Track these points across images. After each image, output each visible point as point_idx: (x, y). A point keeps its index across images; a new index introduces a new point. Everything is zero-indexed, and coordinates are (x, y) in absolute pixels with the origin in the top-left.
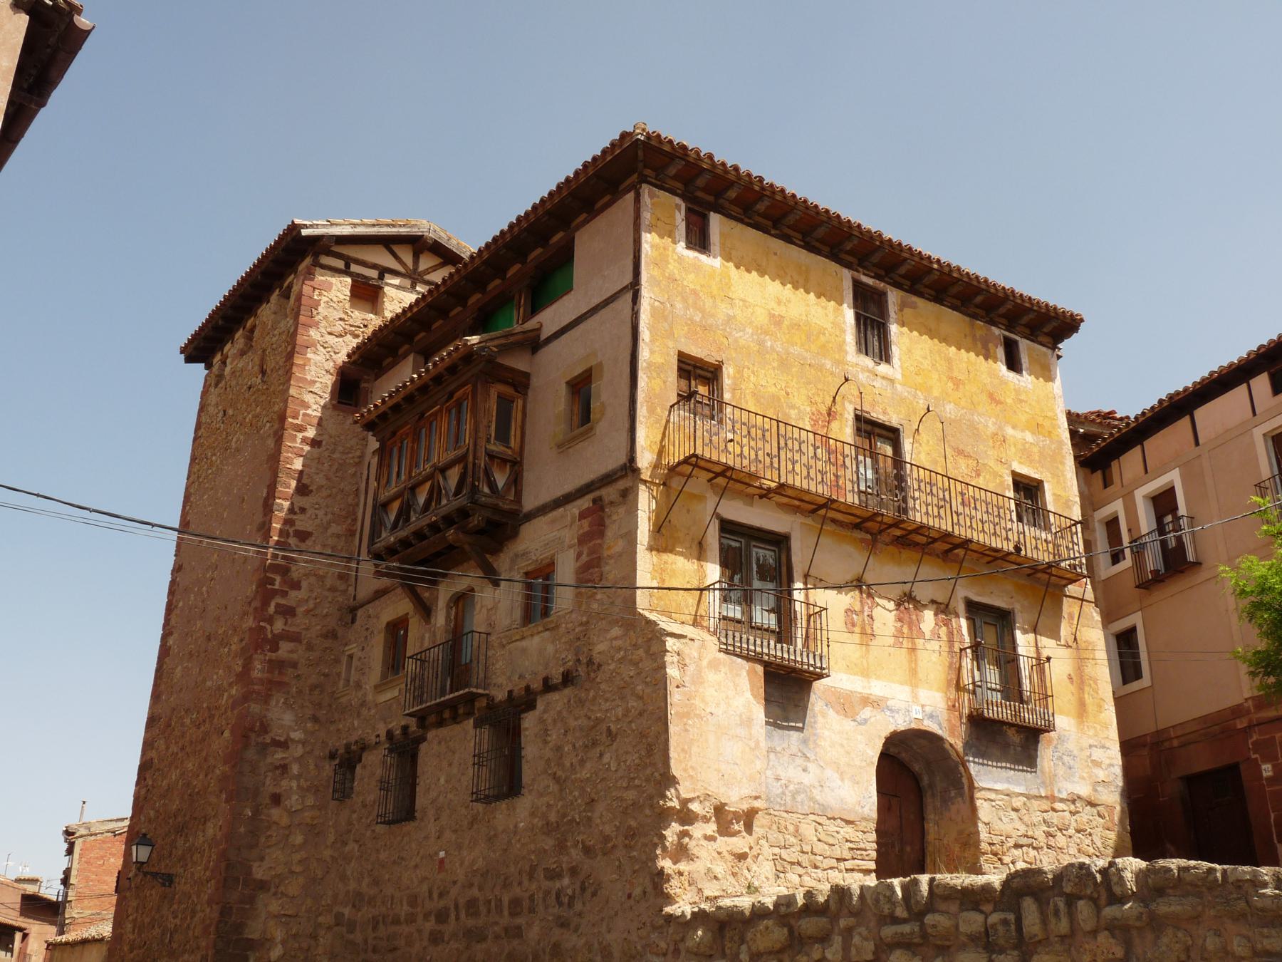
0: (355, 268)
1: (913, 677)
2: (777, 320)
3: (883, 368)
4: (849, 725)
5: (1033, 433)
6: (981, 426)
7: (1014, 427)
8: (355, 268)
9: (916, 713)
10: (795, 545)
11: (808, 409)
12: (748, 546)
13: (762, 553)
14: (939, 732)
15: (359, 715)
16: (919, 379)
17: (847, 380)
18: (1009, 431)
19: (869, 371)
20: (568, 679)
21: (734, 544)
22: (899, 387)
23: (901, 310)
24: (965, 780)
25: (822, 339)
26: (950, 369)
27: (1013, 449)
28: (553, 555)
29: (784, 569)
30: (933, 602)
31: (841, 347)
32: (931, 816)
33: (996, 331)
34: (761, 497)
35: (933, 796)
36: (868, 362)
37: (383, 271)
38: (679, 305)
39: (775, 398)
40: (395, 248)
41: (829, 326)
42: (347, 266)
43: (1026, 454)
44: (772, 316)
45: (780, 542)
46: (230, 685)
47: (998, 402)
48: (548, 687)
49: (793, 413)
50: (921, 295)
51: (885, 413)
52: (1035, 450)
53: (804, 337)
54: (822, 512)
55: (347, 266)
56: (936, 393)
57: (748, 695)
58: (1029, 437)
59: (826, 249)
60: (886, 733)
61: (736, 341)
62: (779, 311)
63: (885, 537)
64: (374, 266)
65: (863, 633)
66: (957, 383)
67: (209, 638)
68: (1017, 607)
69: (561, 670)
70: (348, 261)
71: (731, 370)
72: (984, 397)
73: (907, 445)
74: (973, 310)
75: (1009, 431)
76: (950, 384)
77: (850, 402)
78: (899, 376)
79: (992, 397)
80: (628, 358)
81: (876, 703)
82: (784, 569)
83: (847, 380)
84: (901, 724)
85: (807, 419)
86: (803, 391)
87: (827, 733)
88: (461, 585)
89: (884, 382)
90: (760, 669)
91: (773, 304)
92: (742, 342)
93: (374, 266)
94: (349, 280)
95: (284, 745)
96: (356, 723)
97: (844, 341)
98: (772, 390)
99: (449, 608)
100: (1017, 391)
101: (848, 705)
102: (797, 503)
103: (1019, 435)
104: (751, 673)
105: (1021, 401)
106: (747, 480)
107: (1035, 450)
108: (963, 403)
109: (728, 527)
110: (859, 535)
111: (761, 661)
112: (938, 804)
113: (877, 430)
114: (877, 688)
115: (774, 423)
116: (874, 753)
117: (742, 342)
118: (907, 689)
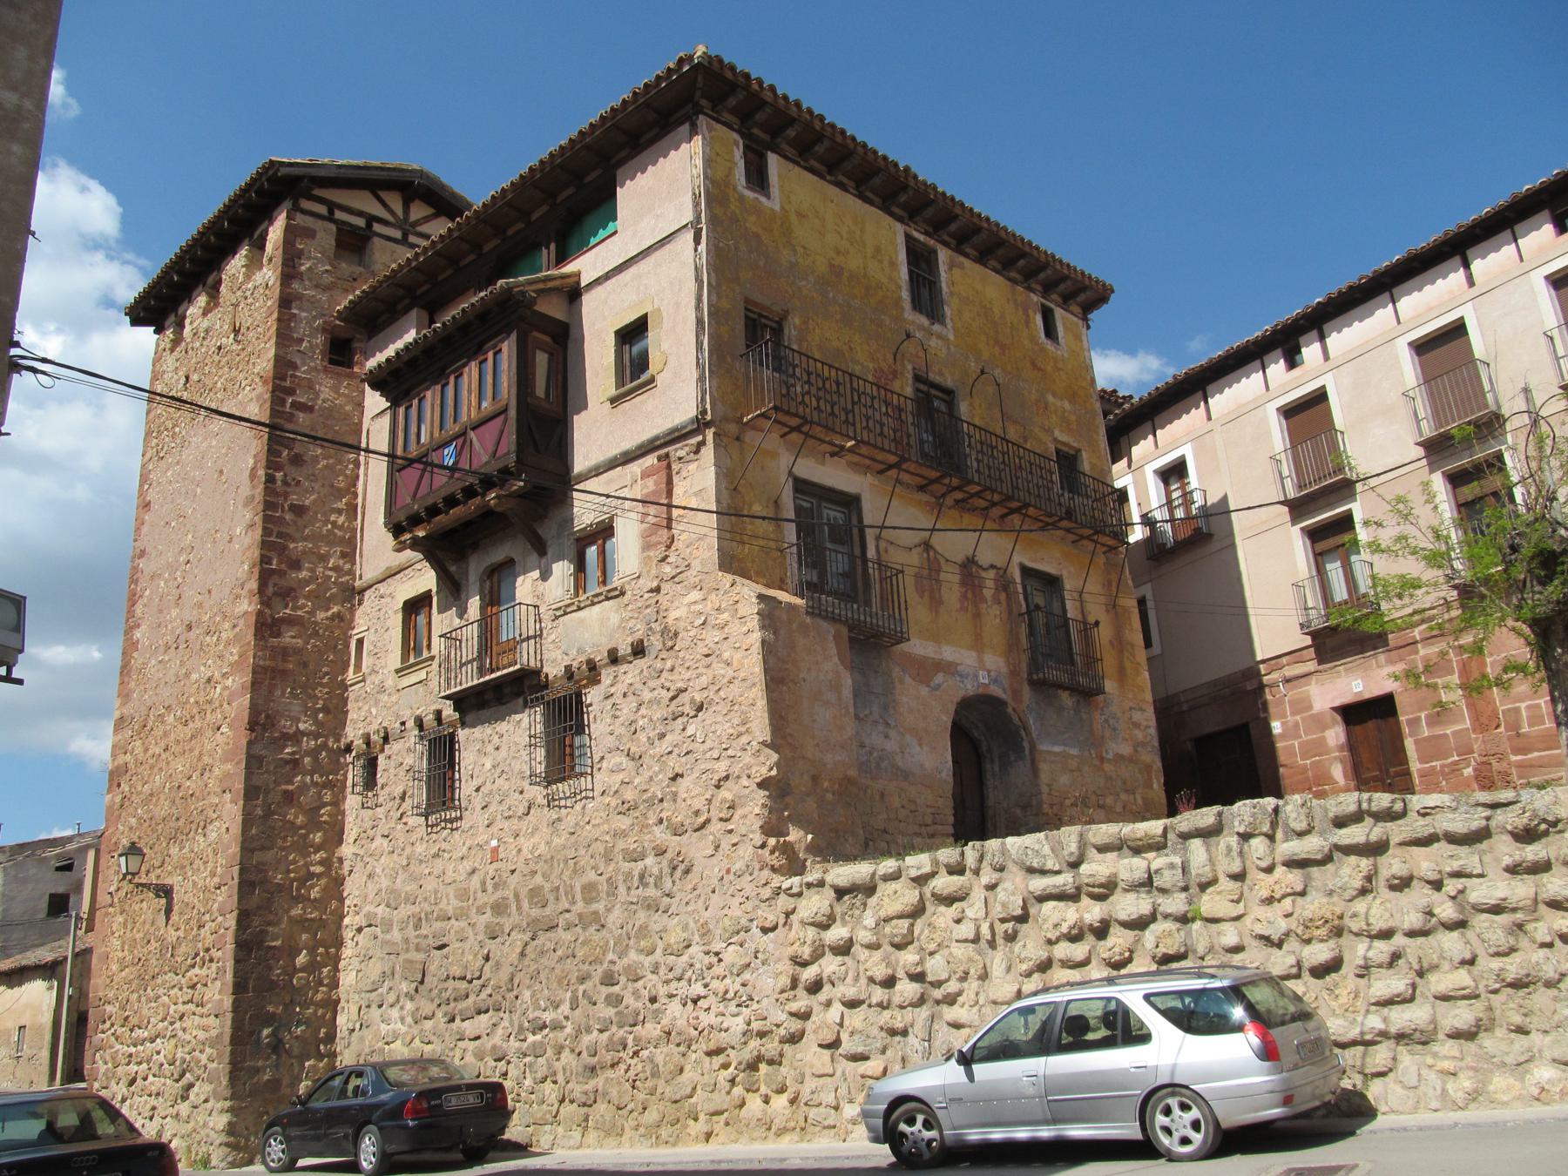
0: (339, 215)
1: (978, 644)
2: (836, 271)
3: (937, 328)
4: (924, 691)
7: (1054, 395)
8: (339, 215)
9: (983, 678)
10: (866, 506)
12: (819, 506)
13: (832, 514)
14: (1004, 696)
15: (377, 702)
17: (908, 336)
18: (1050, 398)
20: (639, 650)
21: (805, 505)
23: (950, 269)
24: (1026, 744)
28: (611, 519)
29: (855, 531)
30: (992, 567)
32: (990, 782)
33: (1035, 298)
34: (833, 455)
35: (992, 761)
36: (924, 320)
37: (371, 219)
38: (743, 248)
40: (382, 194)
41: (885, 280)
42: (331, 212)
44: (832, 266)
45: (850, 502)
46: (224, 675)
48: (614, 658)
50: (966, 255)
51: (941, 374)
52: (1073, 418)
54: (893, 473)
55: (331, 212)
57: (836, 659)
58: (1067, 405)
59: (877, 200)
60: (957, 699)
62: (839, 260)
63: (949, 501)
64: (360, 214)
65: (932, 598)
66: (1003, 347)
67: (189, 627)
68: (1065, 573)
69: (630, 640)
70: (332, 206)
71: (797, 321)
73: (963, 408)
74: (1013, 274)
75: (1050, 398)
78: (952, 337)
80: (693, 303)
81: (949, 668)
82: (855, 531)
83: (908, 336)
84: (969, 688)
87: (905, 699)
88: (498, 555)
90: (844, 630)
91: (832, 254)
92: (805, 292)
93: (360, 214)
94: (333, 227)
95: (296, 737)
96: (374, 711)
98: (836, 344)
99: (482, 581)
100: (1055, 360)
101: (926, 670)
102: (867, 462)
103: (1059, 403)
104: (837, 637)
106: (822, 436)
107: (1073, 418)
109: (802, 487)
110: (924, 497)
111: (845, 623)
112: (997, 769)
113: (933, 392)
114: (948, 653)
115: (847, 378)
116: (947, 720)
117: (805, 292)
118: (974, 654)
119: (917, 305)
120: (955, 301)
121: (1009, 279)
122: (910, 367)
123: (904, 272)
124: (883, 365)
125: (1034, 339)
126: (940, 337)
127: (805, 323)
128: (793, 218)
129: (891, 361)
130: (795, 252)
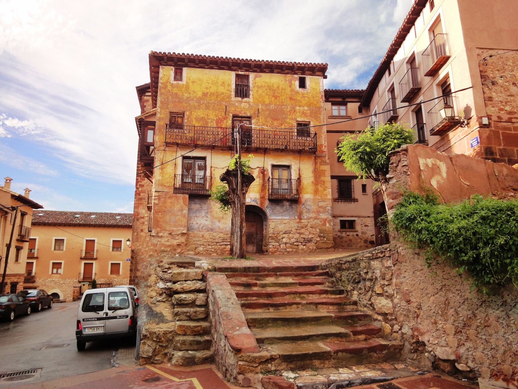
5: (308, 107)
6: (285, 109)
7: (300, 106)
11: (215, 118)
16: (260, 100)
19: (239, 101)
21: (190, 162)
22: (251, 104)
23: (255, 79)
25: (222, 95)
26: (274, 93)
27: (298, 114)
31: (229, 97)
39: (203, 118)
43: (304, 114)
47: (295, 99)
49: (209, 121)
51: (245, 113)
53: (215, 97)
56: (267, 102)
58: (306, 108)
61: (190, 104)
62: (206, 91)
66: (276, 97)
72: (288, 99)
75: (297, 108)
76: (273, 98)
77: (232, 113)
79: (291, 99)
85: (214, 122)
86: (214, 113)
89: (245, 104)
91: (205, 90)
97: (231, 95)
98: (203, 116)
103: (302, 109)
105: (304, 97)
108: (278, 103)
113: (244, 119)
119: (237, 95)
120: (256, 88)
121: (285, 74)
122: (231, 115)
123: (233, 86)
124: (221, 117)
125: (292, 90)
126: (245, 102)
127: (191, 113)
128: (191, 84)
129: (223, 114)
130: (190, 93)
